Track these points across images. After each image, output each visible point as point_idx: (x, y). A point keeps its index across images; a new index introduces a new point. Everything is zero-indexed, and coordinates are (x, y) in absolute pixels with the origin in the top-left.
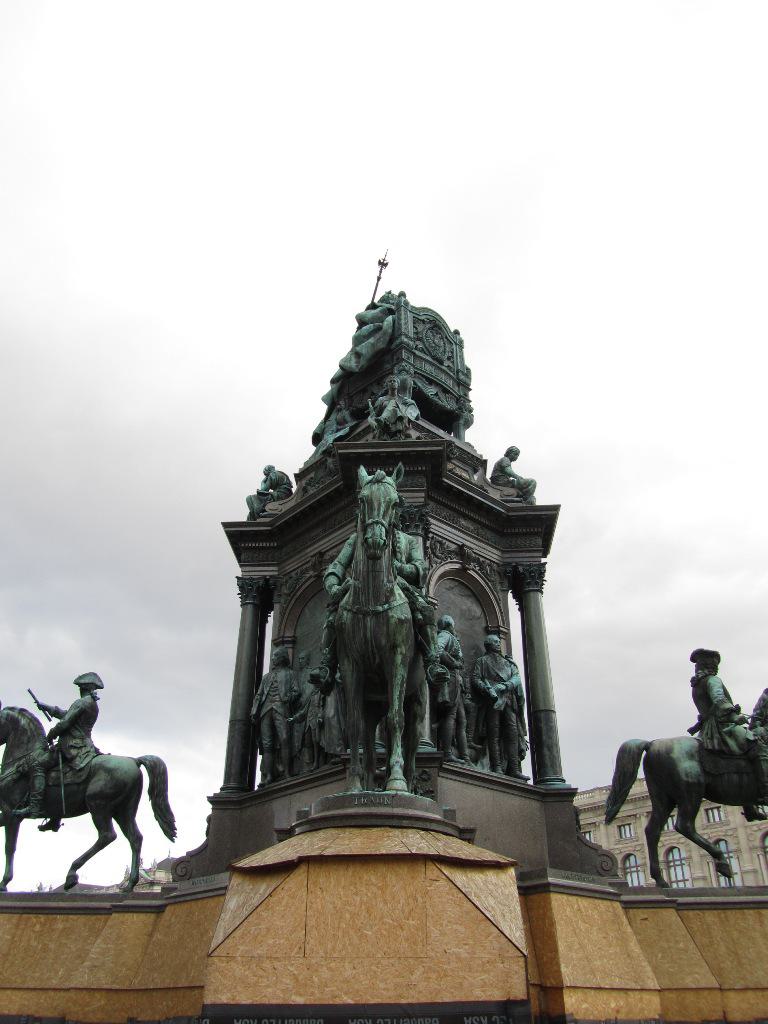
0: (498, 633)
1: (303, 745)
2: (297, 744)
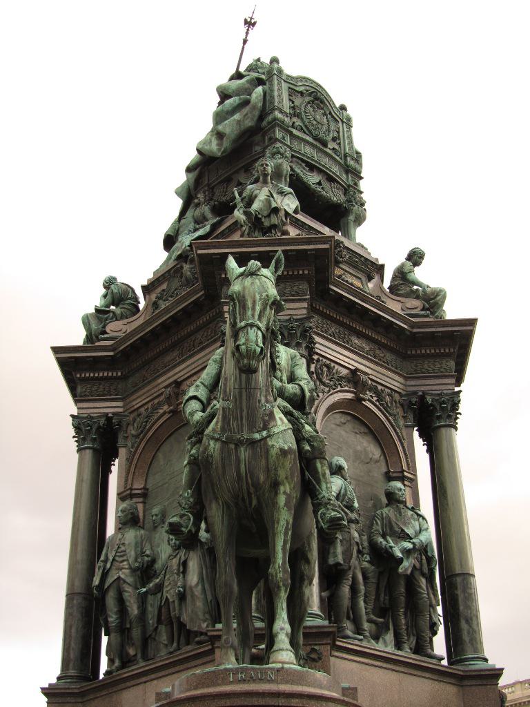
0: (402, 479)
1: (159, 621)
2: (151, 620)
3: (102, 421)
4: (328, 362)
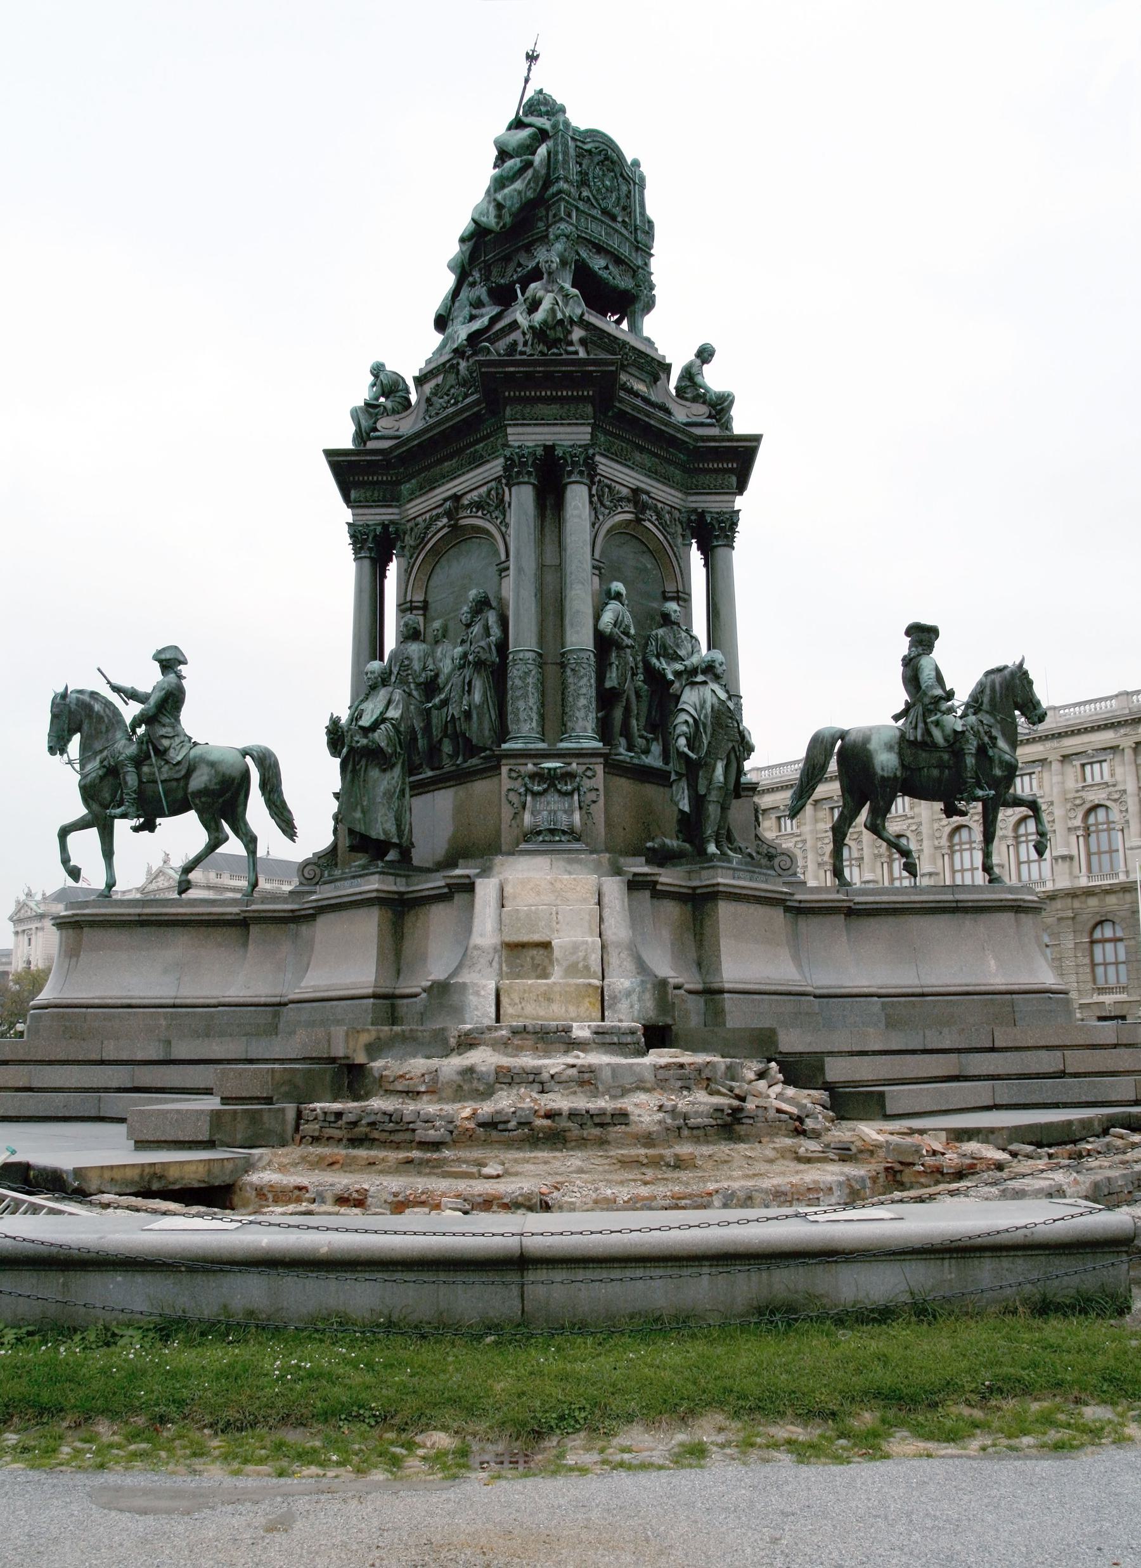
0: (677, 599)
1: (445, 735)
2: (436, 733)
3: (379, 529)
4: (609, 482)
